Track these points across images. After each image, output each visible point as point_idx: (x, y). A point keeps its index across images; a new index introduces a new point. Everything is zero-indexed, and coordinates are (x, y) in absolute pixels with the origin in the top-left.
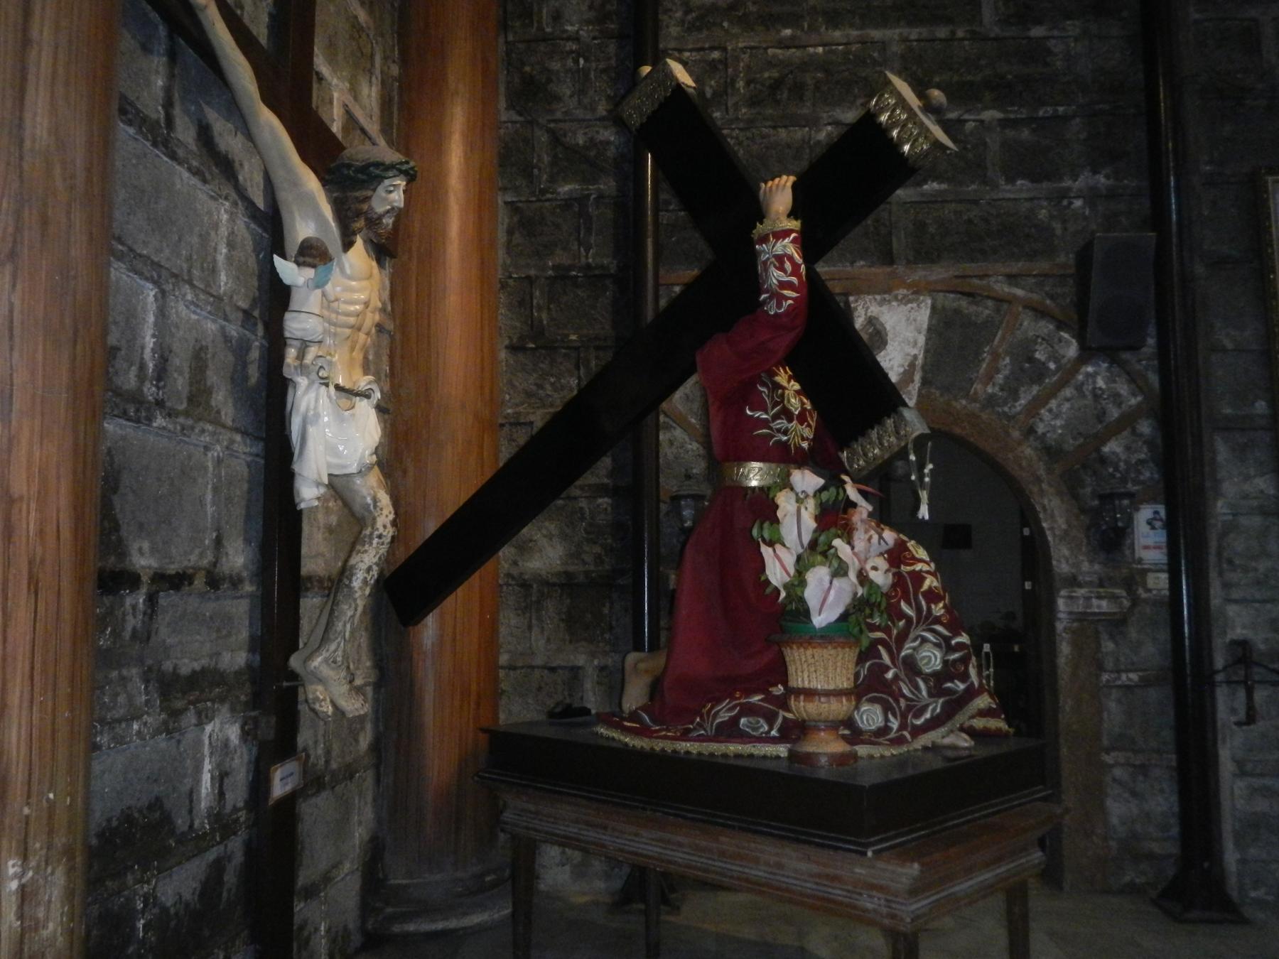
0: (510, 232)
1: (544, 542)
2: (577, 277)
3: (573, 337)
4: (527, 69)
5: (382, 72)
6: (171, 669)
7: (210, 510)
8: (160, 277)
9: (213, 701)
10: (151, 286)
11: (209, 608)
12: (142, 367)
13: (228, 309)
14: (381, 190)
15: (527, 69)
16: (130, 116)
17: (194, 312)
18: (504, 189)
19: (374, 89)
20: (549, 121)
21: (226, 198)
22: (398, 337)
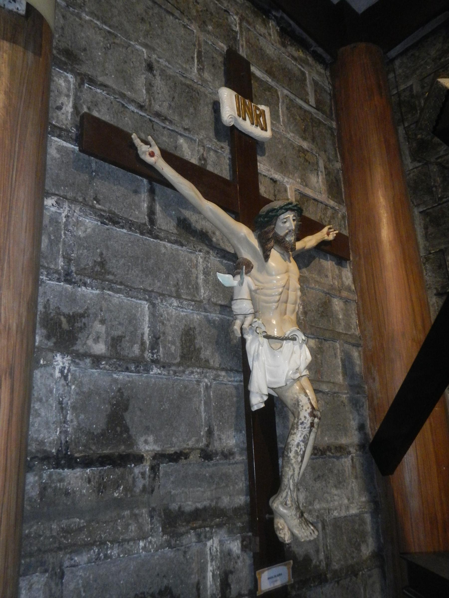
0: (426, 228)
4: (419, 136)
5: (325, 168)
6: (177, 508)
7: (203, 415)
8: (150, 297)
9: (211, 527)
10: (145, 302)
11: (207, 471)
12: (143, 343)
13: (207, 306)
14: (279, 223)
15: (419, 136)
16: (121, 224)
17: (183, 311)
18: (418, 206)
20: (437, 159)
21: (200, 251)
22: (360, 303)
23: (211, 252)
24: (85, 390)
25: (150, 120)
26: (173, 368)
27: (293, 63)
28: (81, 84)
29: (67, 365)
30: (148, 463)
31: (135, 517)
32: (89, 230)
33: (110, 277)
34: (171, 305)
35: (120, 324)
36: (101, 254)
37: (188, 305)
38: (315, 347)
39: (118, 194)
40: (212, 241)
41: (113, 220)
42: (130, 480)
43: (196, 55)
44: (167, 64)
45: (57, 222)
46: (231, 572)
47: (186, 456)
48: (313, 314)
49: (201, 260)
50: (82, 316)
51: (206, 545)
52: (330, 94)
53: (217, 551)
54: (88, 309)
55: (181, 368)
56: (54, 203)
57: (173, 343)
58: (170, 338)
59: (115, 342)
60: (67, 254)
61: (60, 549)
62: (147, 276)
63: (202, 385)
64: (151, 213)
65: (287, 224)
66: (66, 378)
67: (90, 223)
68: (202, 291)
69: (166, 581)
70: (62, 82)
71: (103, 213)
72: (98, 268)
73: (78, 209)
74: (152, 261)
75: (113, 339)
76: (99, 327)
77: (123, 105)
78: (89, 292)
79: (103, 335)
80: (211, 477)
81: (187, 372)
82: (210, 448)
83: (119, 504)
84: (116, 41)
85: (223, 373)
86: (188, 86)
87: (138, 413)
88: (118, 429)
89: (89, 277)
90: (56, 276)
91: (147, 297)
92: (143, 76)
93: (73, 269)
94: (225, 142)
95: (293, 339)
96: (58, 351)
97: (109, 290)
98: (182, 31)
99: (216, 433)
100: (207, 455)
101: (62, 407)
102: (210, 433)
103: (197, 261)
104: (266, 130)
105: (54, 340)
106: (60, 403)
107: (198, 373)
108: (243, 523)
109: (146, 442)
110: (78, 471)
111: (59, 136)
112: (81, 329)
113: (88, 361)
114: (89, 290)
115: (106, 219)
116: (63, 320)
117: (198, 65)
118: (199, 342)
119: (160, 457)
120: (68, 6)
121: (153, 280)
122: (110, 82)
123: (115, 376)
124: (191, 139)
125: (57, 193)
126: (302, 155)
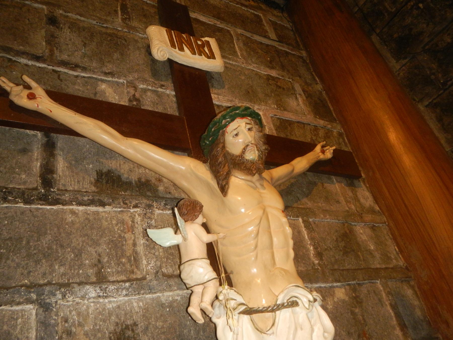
0: (440, 120)
4: (395, 36)
5: (304, 91)
10: (31, 306)
14: (229, 138)
17: (110, 302)
18: (421, 101)
19: (300, 100)
21: (136, 206)
22: (392, 225)
23: (155, 204)
25: (53, 70)
27: (244, 10)
37: (117, 290)
38: (347, 298)
40: (157, 190)
43: (119, 8)
44: (79, 17)
48: (331, 253)
49: (138, 219)
52: (292, 30)
62: (37, 262)
68: (145, 262)
86: (110, 35)
91: (34, 296)
95: (293, 304)
103: (133, 222)
104: (214, 58)
121: (51, 266)
126: (271, 82)
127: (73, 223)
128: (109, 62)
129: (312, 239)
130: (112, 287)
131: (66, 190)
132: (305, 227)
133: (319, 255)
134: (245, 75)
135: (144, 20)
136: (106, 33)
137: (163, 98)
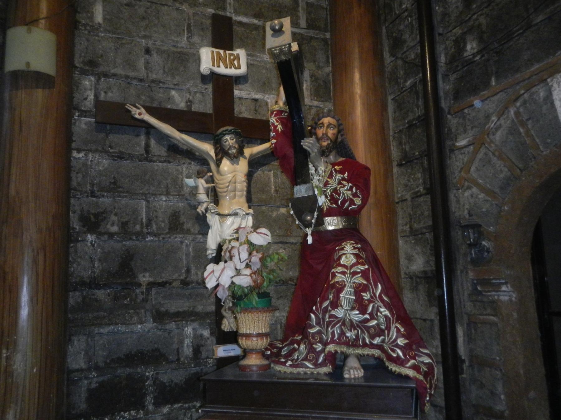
1: (416, 256)
2: (416, 123)
3: (417, 154)
4: (394, 35)
7: (184, 261)
8: (146, 197)
9: (187, 321)
11: (187, 292)
12: (142, 224)
13: (189, 197)
15: (394, 35)
20: (403, 54)
21: (184, 164)
24: (106, 251)
25: (149, 86)
26: (163, 236)
28: (98, 80)
29: (94, 239)
30: (145, 287)
31: (138, 314)
32: (106, 165)
33: (121, 189)
34: (161, 200)
35: (127, 214)
36: (114, 178)
39: (125, 140)
41: (121, 156)
42: (134, 295)
45: (87, 165)
46: (203, 346)
47: (170, 284)
49: (184, 169)
50: (103, 213)
51: (184, 330)
53: (190, 333)
54: (106, 208)
55: (168, 236)
56: (84, 155)
57: (163, 221)
58: (161, 219)
59: (124, 225)
60: (92, 182)
61: (93, 325)
62: (145, 185)
63: (184, 244)
64: (147, 146)
65: (227, 143)
66: (93, 246)
67: (106, 162)
69: (156, 346)
70: (87, 83)
71: (114, 155)
72: (112, 186)
73: (98, 155)
74: (148, 176)
75: (122, 223)
76: (114, 218)
77: (129, 83)
78: (106, 201)
79: (117, 222)
80: (190, 295)
81: (172, 238)
82: (188, 279)
83: (126, 306)
84: (124, 41)
85: (200, 236)
87: (140, 261)
88: (127, 270)
89: (106, 192)
90: (86, 194)
92: (143, 59)
93: (95, 189)
94: (210, 83)
95: (236, 214)
96: (89, 233)
97: (118, 197)
98: (175, 14)
99: (193, 272)
100: (185, 283)
101: (92, 260)
102: (188, 271)
104: (240, 68)
105: (87, 227)
106: (91, 258)
107: (180, 238)
108: (211, 320)
109: (144, 276)
110: (102, 291)
111: (85, 116)
112: (103, 220)
113: (106, 237)
114: (105, 199)
115: (116, 157)
116: (92, 217)
117: (187, 35)
118: (183, 219)
119: (151, 285)
120: (89, 32)
122: (119, 71)
123: (124, 243)
124: (181, 90)
125: (86, 148)
127: (157, 170)
128: (177, 75)
129: (275, 182)
130: (172, 197)
131: (155, 155)
132: (274, 176)
133: (276, 191)
134: (266, 69)
135: (202, 33)
136: (177, 52)
137: (204, 103)
